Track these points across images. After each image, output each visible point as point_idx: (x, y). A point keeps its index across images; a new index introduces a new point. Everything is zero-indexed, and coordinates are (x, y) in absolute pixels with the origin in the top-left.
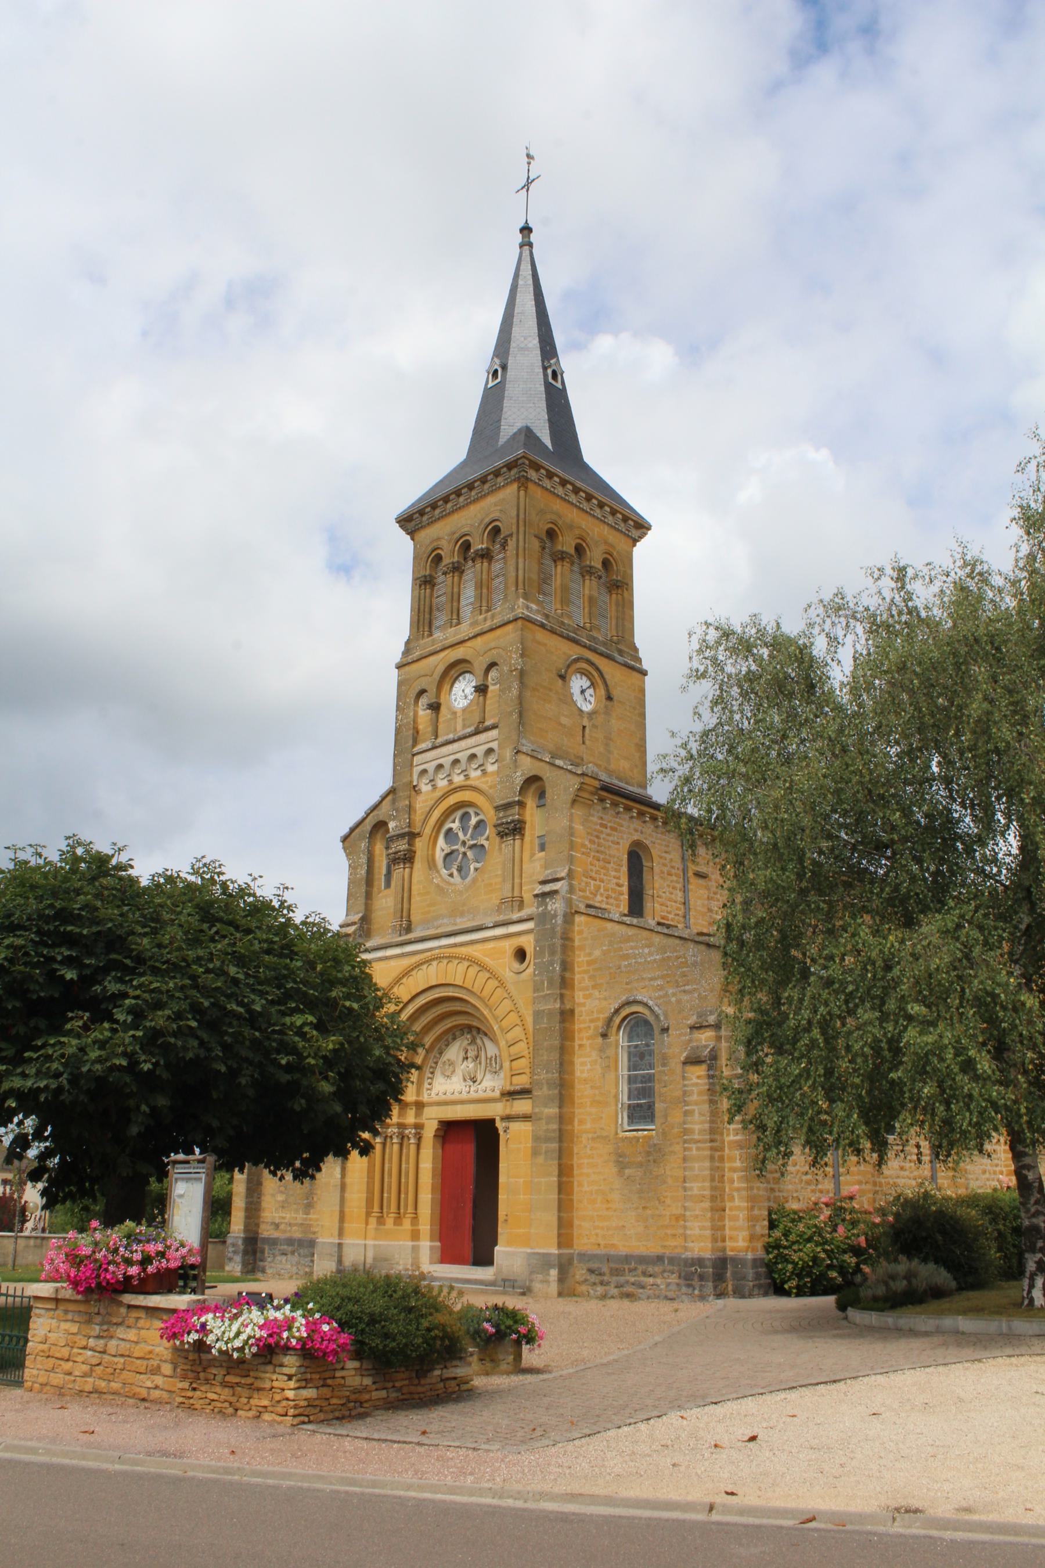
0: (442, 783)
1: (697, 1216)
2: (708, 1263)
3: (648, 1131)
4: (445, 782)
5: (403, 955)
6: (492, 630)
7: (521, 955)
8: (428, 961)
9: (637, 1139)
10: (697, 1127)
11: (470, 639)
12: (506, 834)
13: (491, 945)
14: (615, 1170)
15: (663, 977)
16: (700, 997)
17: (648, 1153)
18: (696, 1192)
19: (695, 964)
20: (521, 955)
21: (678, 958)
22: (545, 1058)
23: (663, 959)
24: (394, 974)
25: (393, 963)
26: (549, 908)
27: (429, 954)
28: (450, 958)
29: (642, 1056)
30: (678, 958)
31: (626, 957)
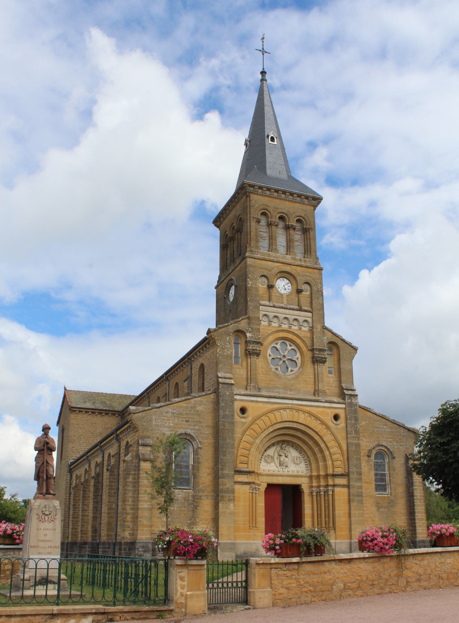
0: (275, 324)
1: (420, 526)
2: (426, 542)
3: (385, 495)
4: (276, 325)
5: (268, 402)
6: (307, 267)
7: (336, 417)
8: (284, 409)
9: (385, 497)
10: (419, 494)
11: (294, 265)
12: (321, 362)
13: (321, 409)
14: (375, 509)
15: (391, 438)
16: (406, 448)
17: (389, 503)
18: (420, 517)
19: (404, 436)
20: (336, 417)
21: (397, 432)
22: (355, 462)
23: (392, 431)
24: (265, 410)
25: (260, 405)
26: (353, 401)
27: (285, 406)
28: (298, 410)
29: (380, 466)
30: (397, 432)
31: (377, 427)
